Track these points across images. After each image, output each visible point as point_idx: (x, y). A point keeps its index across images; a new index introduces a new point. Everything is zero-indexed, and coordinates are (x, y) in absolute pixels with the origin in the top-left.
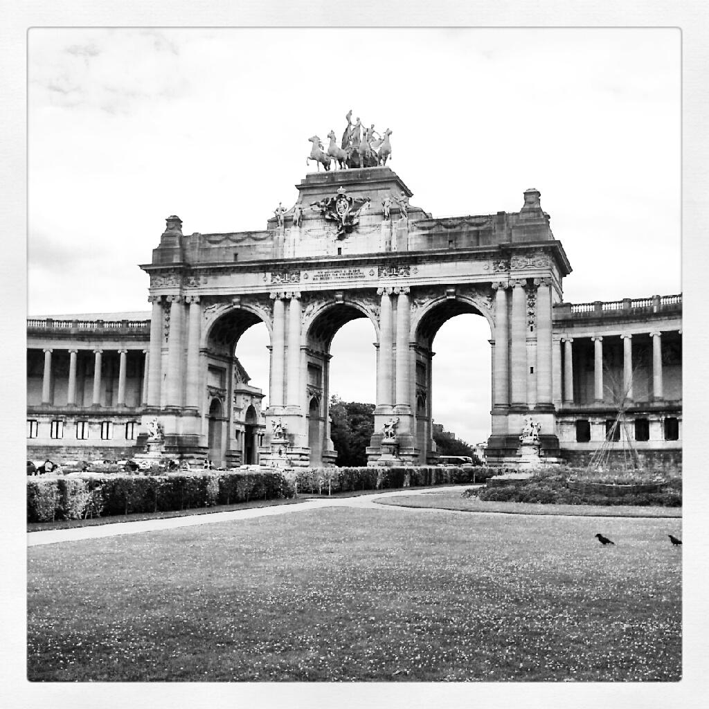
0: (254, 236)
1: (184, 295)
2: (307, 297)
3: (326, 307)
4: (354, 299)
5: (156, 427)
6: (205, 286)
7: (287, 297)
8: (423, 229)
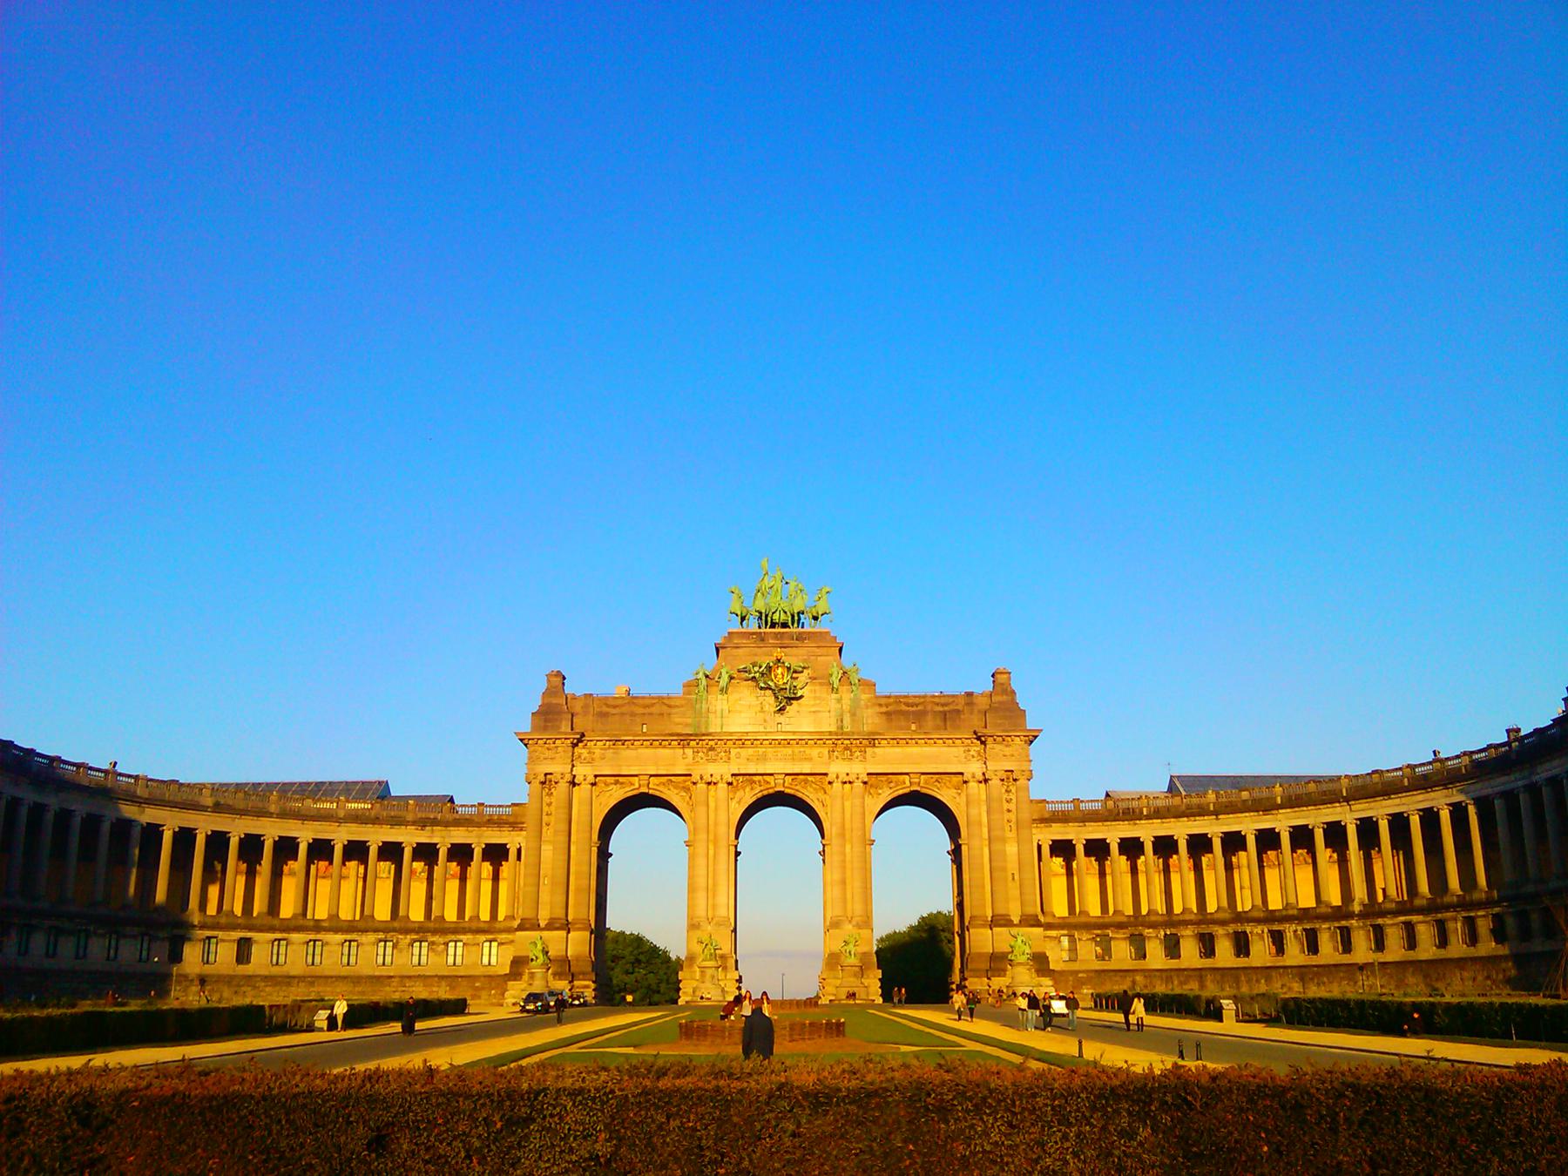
0: (665, 701)
8: (880, 705)
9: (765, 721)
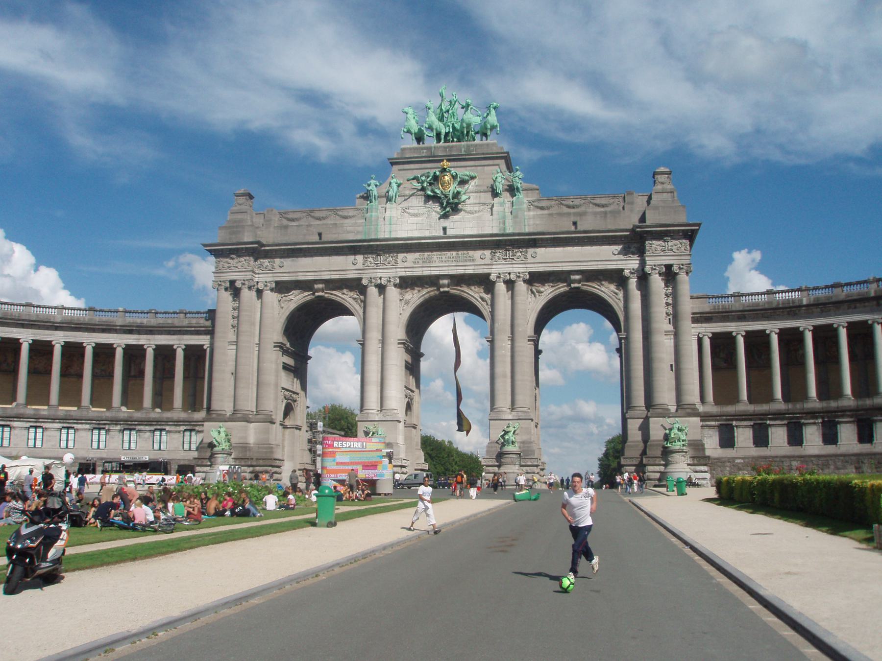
0: (340, 213)
1: (256, 280)
2: (406, 283)
3: (428, 295)
4: (461, 287)
5: (223, 434)
6: (282, 270)
7: (383, 282)
8: (542, 208)
9: (431, 226)
